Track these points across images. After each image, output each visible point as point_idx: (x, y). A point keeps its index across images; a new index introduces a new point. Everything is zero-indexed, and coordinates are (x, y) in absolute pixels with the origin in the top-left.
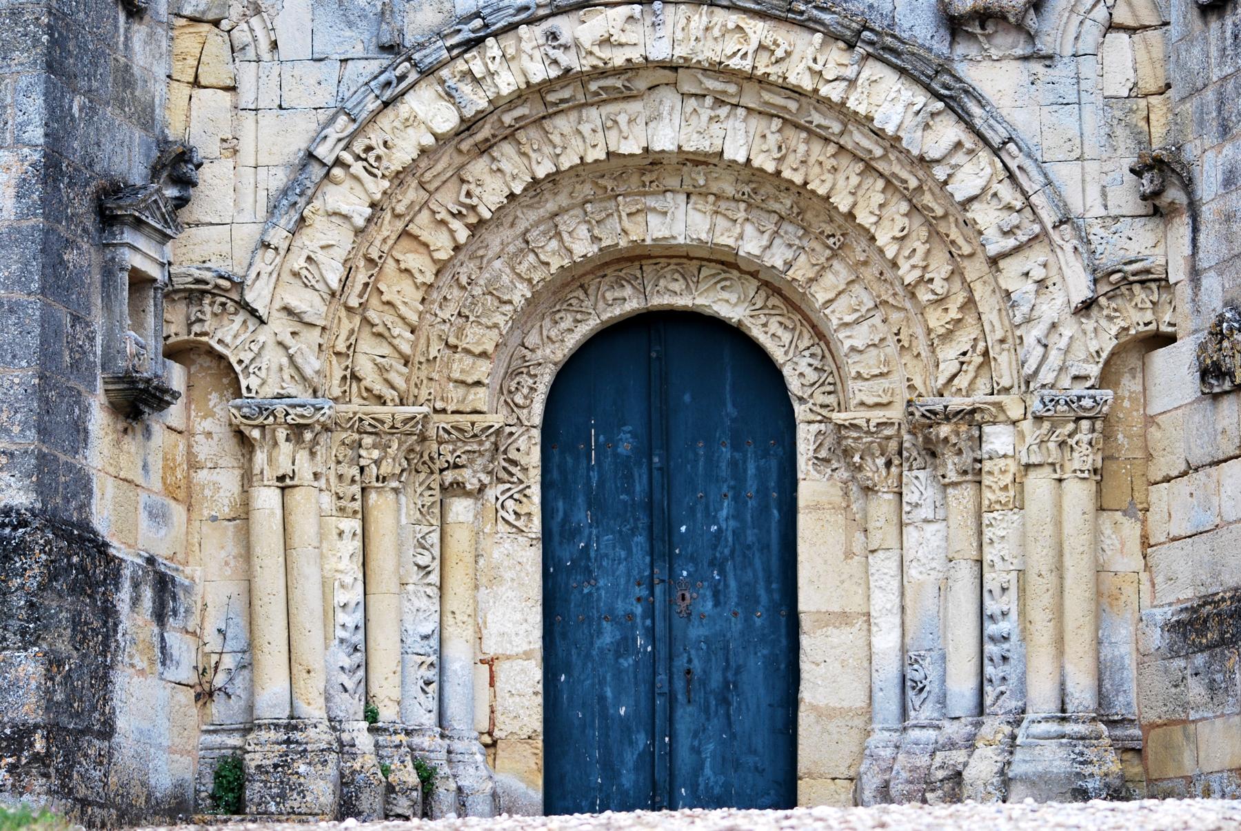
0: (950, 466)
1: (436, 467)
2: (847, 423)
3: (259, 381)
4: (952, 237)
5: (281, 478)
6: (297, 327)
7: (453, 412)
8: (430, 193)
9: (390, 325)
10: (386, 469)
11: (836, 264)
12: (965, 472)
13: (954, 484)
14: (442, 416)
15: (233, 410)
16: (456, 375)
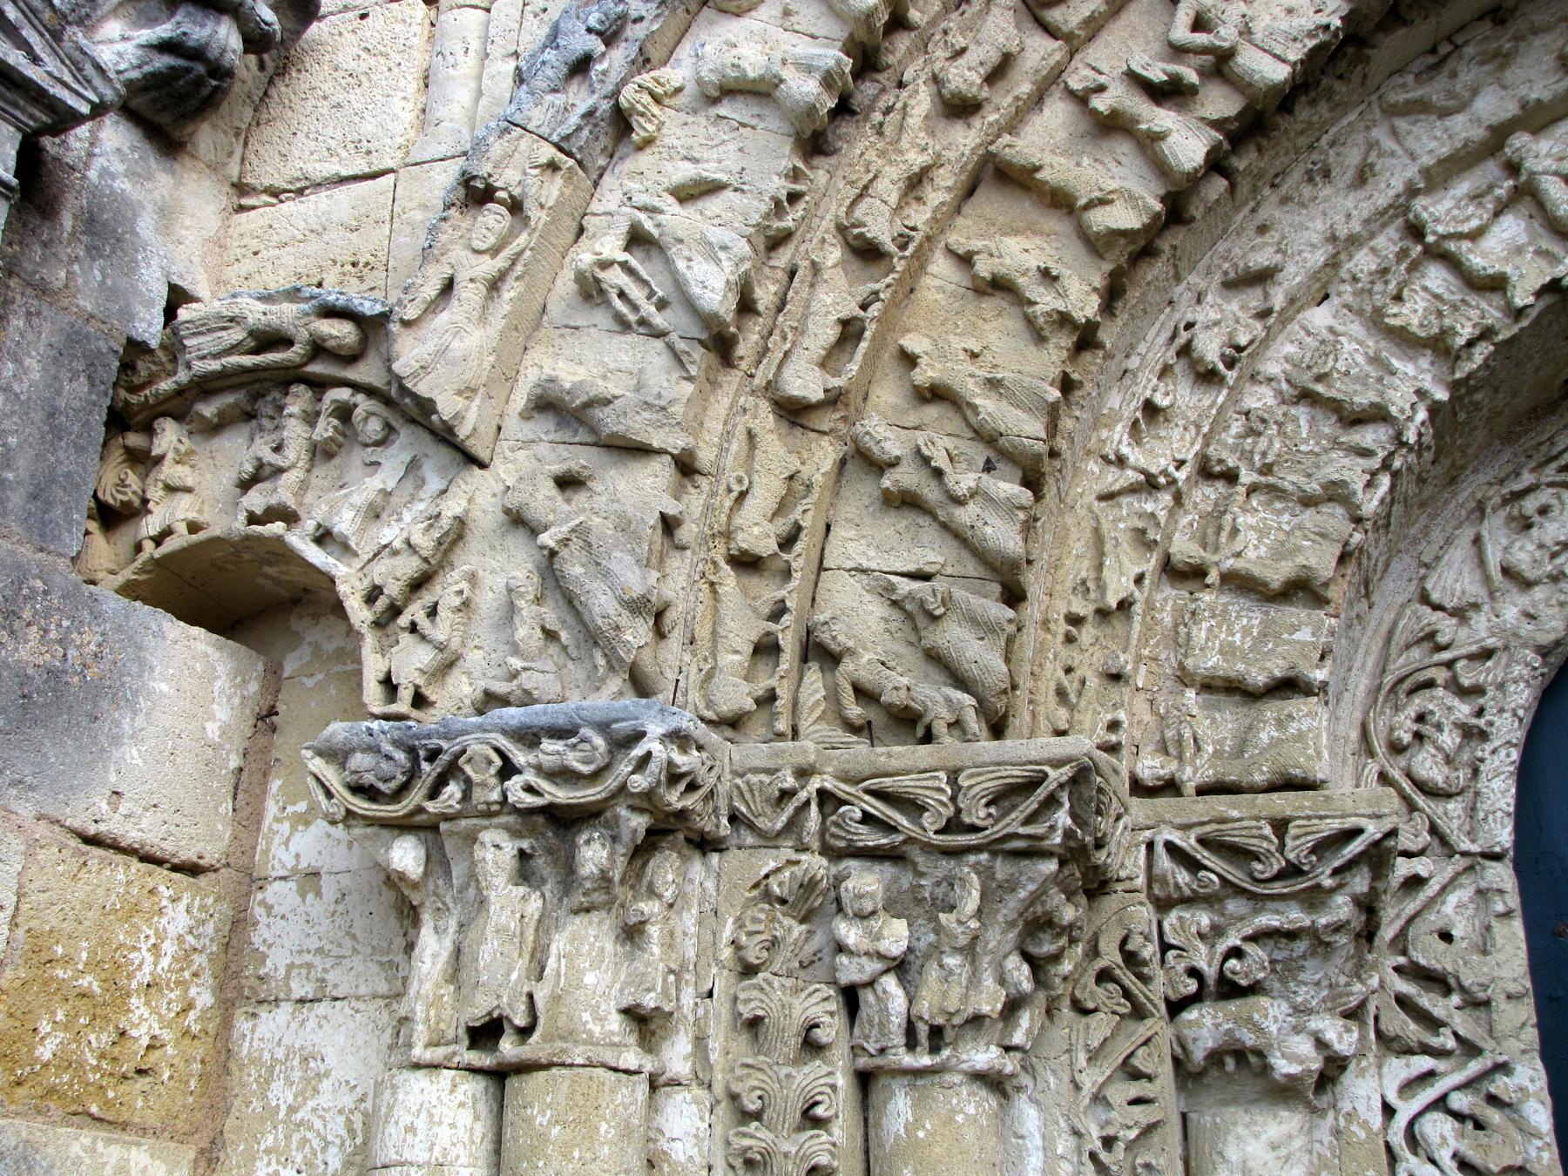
1: (1157, 992)
3: (424, 656)
5: (486, 1033)
6: (578, 459)
7: (1202, 791)
8: (1074, 43)
9: (941, 461)
10: (945, 990)
14: (1163, 805)
15: (317, 765)
16: (1210, 662)
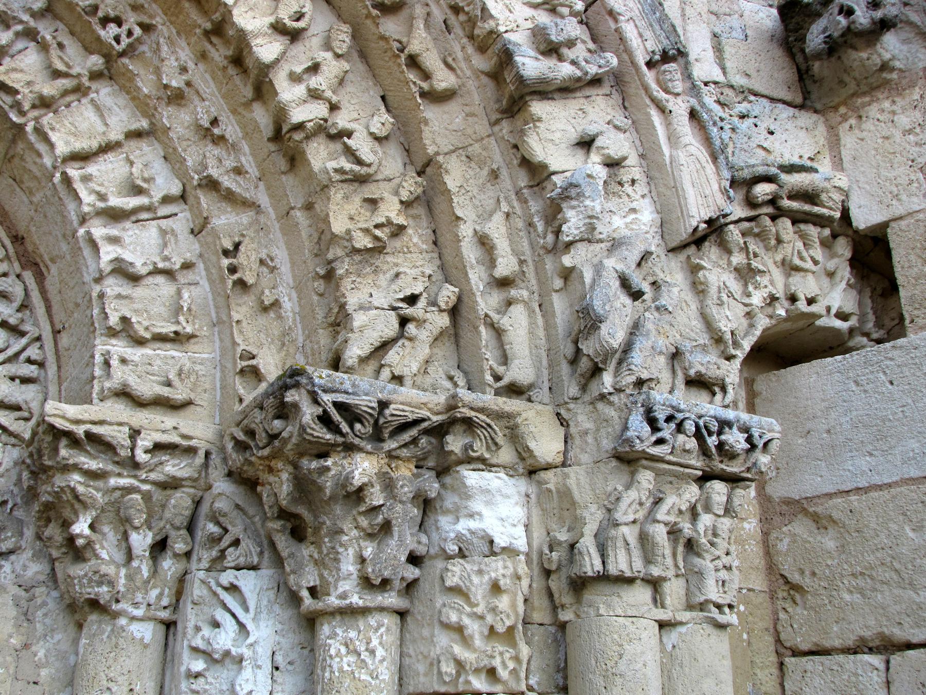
0: (349, 566)
2: (80, 430)
4: (415, 47)
11: (104, 93)
12: (385, 584)
13: (351, 613)
